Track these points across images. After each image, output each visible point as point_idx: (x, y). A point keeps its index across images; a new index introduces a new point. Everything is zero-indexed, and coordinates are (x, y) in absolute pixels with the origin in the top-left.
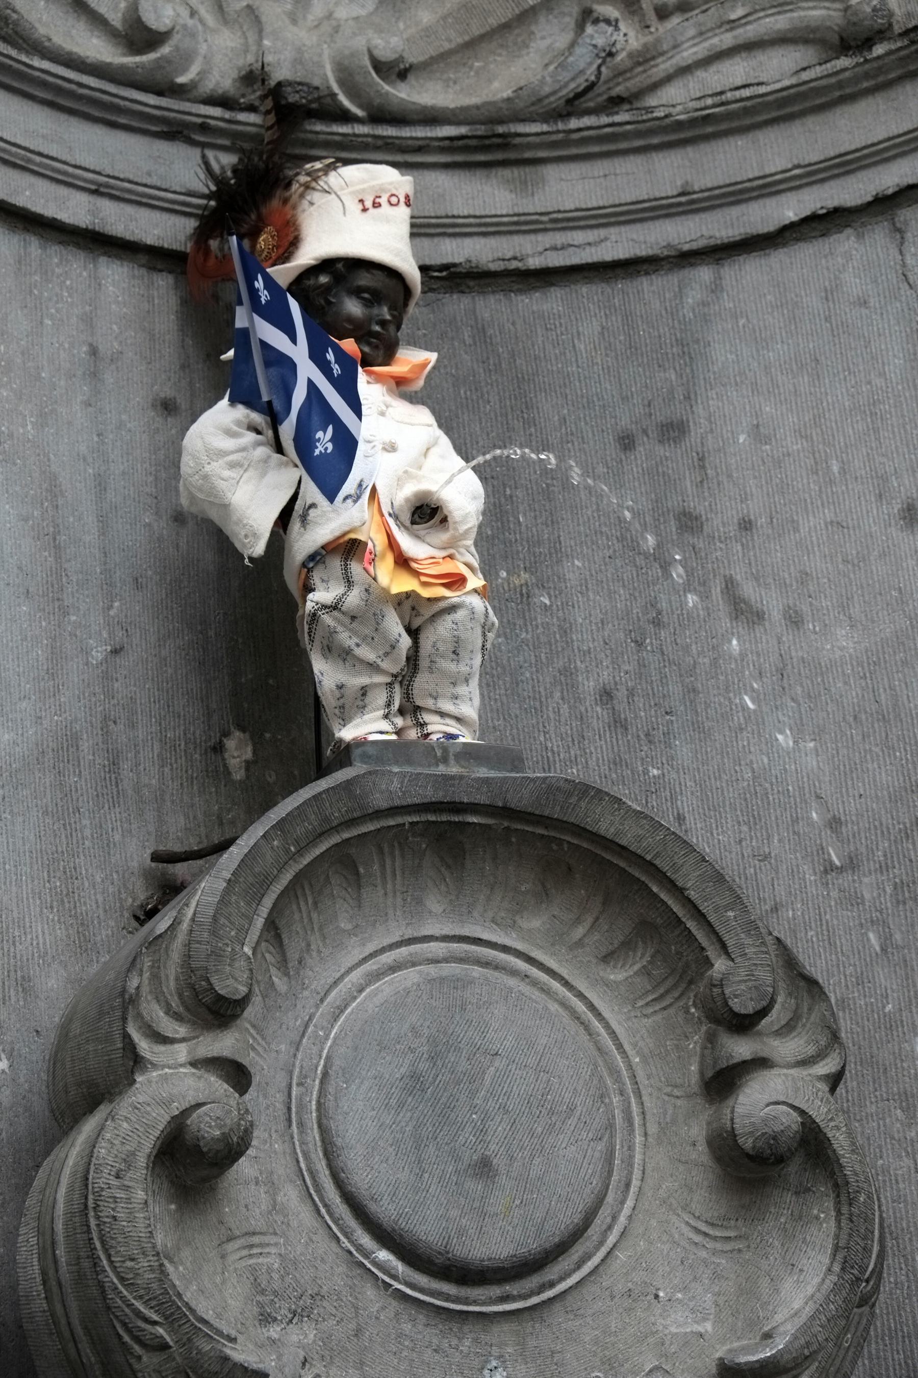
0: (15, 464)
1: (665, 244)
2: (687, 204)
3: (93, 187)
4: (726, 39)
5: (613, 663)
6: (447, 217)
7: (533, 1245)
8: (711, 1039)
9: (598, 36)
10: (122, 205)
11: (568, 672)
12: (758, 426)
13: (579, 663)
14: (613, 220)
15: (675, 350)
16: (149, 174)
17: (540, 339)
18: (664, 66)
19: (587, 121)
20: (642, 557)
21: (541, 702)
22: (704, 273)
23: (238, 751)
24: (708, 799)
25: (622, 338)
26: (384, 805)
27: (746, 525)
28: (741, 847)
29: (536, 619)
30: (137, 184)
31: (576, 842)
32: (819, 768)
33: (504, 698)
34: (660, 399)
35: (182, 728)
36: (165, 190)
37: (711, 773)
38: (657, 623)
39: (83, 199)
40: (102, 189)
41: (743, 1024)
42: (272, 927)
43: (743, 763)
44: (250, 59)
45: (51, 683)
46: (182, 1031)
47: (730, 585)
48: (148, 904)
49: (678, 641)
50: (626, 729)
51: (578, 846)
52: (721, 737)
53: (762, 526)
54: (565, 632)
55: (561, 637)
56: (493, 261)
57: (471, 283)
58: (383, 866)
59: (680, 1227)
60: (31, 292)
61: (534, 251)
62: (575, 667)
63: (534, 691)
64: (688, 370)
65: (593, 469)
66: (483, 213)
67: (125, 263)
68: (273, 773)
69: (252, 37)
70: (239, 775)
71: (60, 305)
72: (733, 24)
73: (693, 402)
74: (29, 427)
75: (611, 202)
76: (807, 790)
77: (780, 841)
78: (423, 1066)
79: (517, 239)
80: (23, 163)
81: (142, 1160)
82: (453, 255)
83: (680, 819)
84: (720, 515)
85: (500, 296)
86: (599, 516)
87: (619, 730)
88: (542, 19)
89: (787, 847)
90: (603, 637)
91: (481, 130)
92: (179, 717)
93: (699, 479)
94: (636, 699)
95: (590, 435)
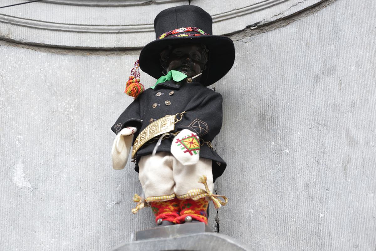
0: (78, 142)
3: (117, 31)
5: (309, 172)
6: (255, 4)
10: (130, 34)
11: (293, 179)
12: (358, 61)
13: (298, 174)
15: (334, 36)
16: (140, 20)
17: (290, 44)
21: (284, 193)
24: (339, 224)
25: (317, 36)
27: (353, 105)
28: (349, 243)
29: (284, 159)
30: (134, 25)
32: (374, 205)
33: (271, 194)
34: (329, 58)
35: (144, 227)
36: (147, 24)
38: (324, 153)
39: (115, 35)
40: (121, 31)
43: (351, 207)
45: (88, 220)
47: (348, 131)
49: (331, 159)
50: (313, 199)
53: (358, 104)
54: (293, 162)
55: (292, 165)
56: (273, 17)
57: (266, 28)
60: (91, 76)
62: (296, 176)
65: (306, 93)
67: (134, 56)
71: (104, 79)
74: (86, 127)
76: (370, 215)
77: (362, 238)
79: (280, 5)
80: (86, 31)
82: (258, 19)
83: (330, 234)
84: (345, 102)
85: (277, 30)
86: (307, 112)
87: (311, 199)
89: (364, 241)
90: (306, 162)
92: (143, 223)
94: (316, 186)
95: (305, 80)
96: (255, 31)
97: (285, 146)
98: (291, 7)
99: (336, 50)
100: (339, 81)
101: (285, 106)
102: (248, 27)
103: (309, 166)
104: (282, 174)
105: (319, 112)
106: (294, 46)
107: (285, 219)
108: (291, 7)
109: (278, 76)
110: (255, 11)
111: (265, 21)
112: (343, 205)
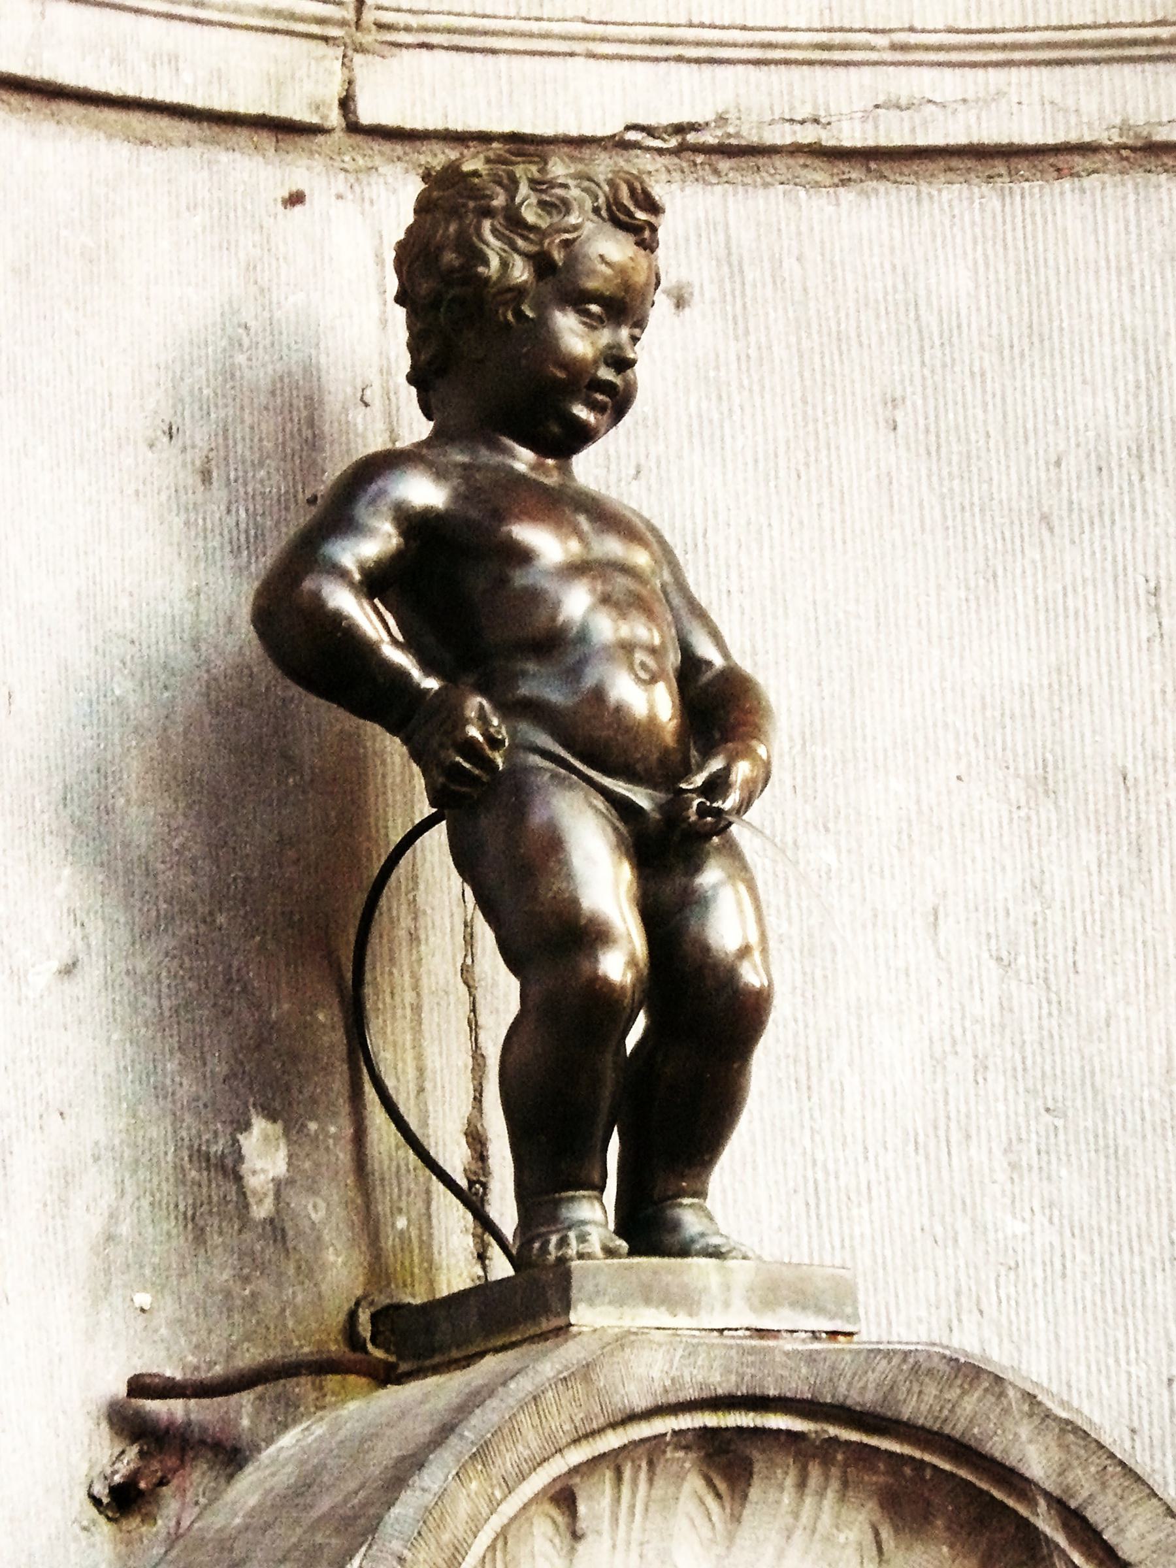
1: (1118, 121)
14: (1017, 55)
15: (1118, 348)
20: (1021, 783)
26: (641, 1403)
31: (947, 1466)
37: (1124, 1240)
48: (114, 1473)
49: (1081, 966)
51: (952, 1475)
52: (1150, 1171)
58: (617, 1500)
61: (851, 109)
63: (796, 1045)
64: (1143, 398)
65: (939, 586)
66: (759, 24)
68: (322, 1205)
70: (261, 1211)
73: (1146, 468)
75: (1018, 23)
93: (1144, 635)
94: (990, 1076)
96: (662, 161)
97: (815, 826)
98: (877, 106)
99: (1128, 426)
100: (1142, 592)
101: (822, 620)
103: (949, 971)
104: (798, 966)
105: (1017, 711)
106: (878, 316)
107: (812, 1202)
108: (877, 106)
109: (782, 449)
110: (679, 59)
111: (731, 130)
112: (1142, 1209)
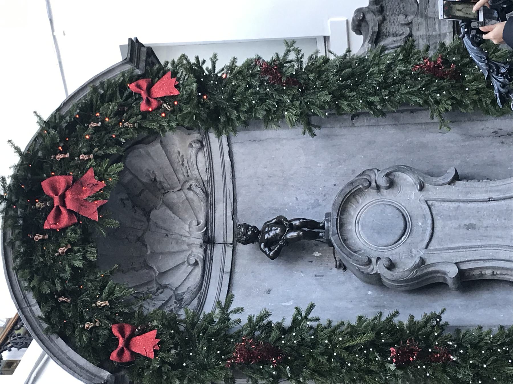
2: (224, 175)
4: (195, 166)
7: (401, 218)
8: (373, 188)
9: (193, 186)
18: (199, 177)
19: (209, 191)
22: (237, 174)
23: (317, 254)
41: (370, 183)
42: (355, 252)
44: (198, 246)
46: (372, 266)
59: (398, 195)
61: (230, 201)
69: (194, 245)
72: (193, 165)
78: (375, 231)
81: (392, 273)
88: (187, 196)
91: (209, 208)
102: (232, 219)
